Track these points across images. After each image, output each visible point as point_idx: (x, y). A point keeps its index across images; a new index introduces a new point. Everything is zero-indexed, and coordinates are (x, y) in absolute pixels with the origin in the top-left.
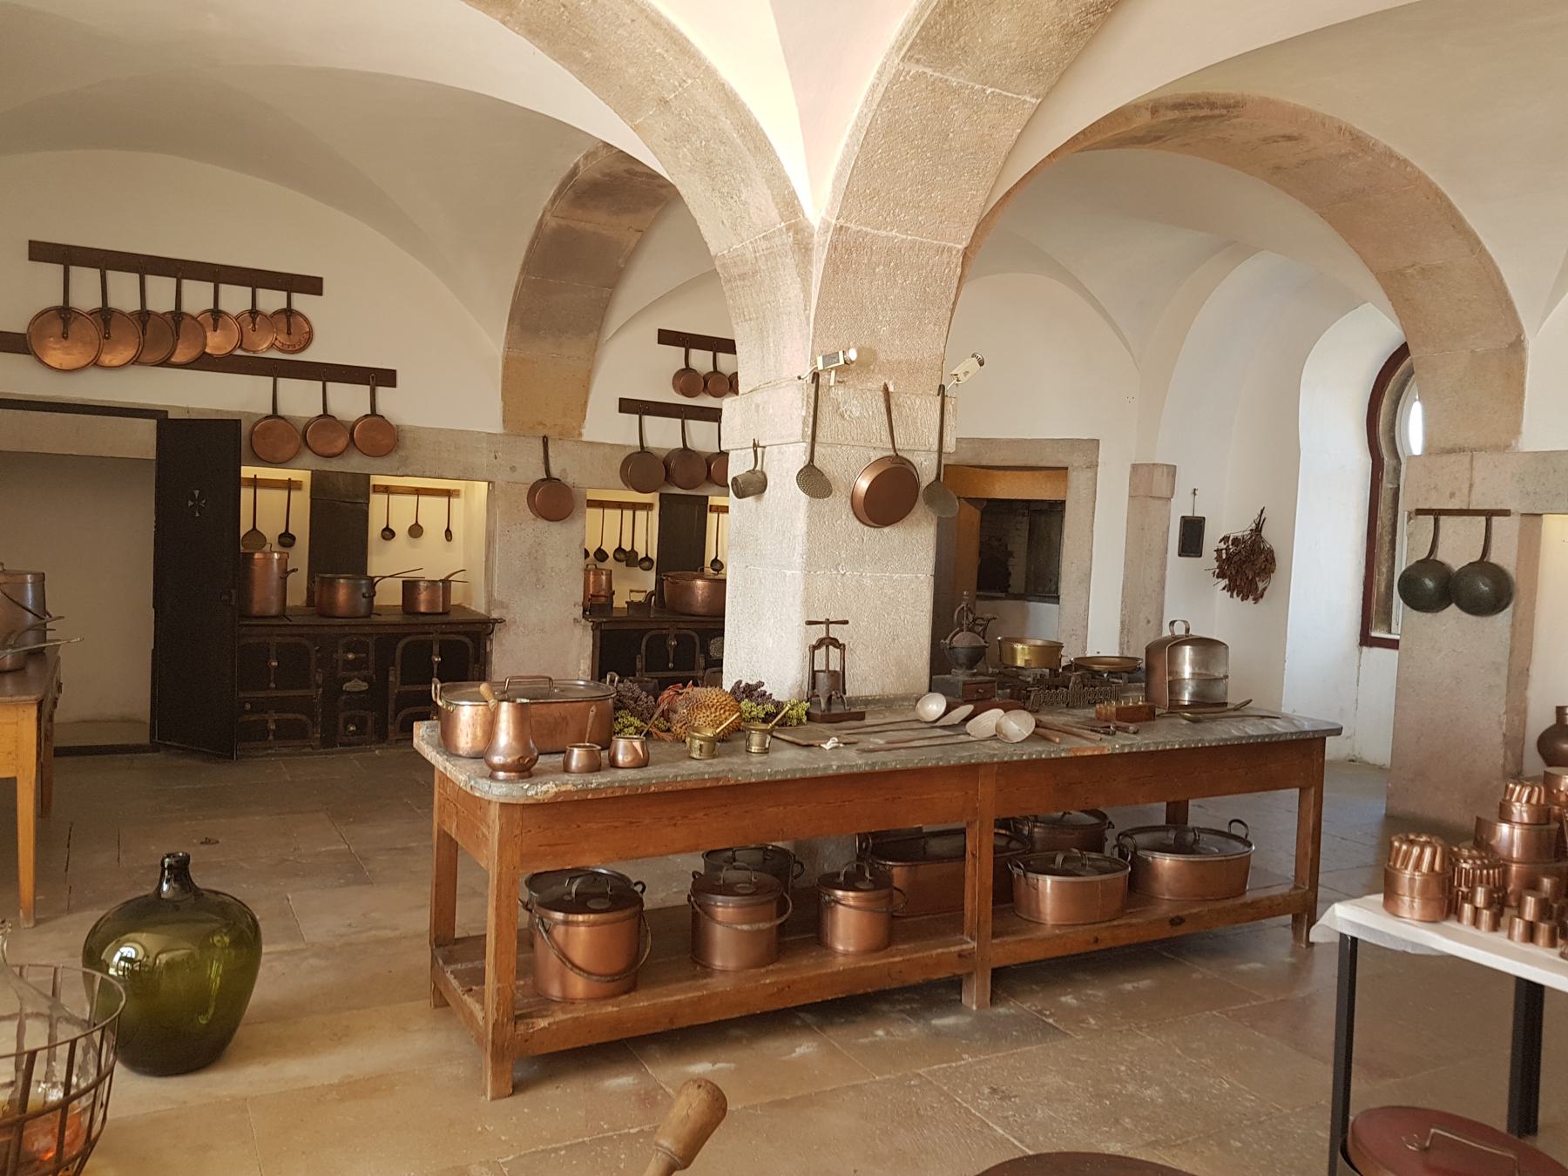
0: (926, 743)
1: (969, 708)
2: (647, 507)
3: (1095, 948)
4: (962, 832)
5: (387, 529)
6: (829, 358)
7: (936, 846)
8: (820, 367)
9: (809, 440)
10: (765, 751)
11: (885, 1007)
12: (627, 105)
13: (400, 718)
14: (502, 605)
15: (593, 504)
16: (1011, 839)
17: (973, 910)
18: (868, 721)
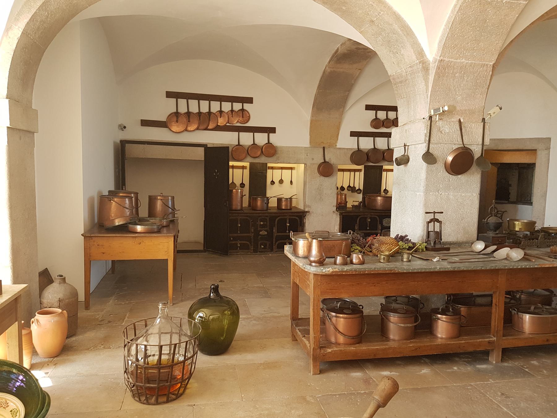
0: (476, 260)
1: (494, 247)
2: (359, 170)
4: (491, 296)
5: (272, 181)
6: (436, 110)
7: (479, 300)
8: (432, 114)
9: (427, 142)
10: (409, 261)
11: (457, 359)
12: (358, 25)
13: (277, 243)
14: (309, 207)
15: (340, 170)
16: (511, 299)
17: (495, 326)
18: (451, 251)
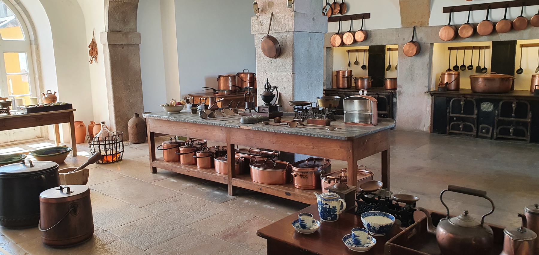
2: (487, 47)
3: (260, 191)
14: (400, 87)
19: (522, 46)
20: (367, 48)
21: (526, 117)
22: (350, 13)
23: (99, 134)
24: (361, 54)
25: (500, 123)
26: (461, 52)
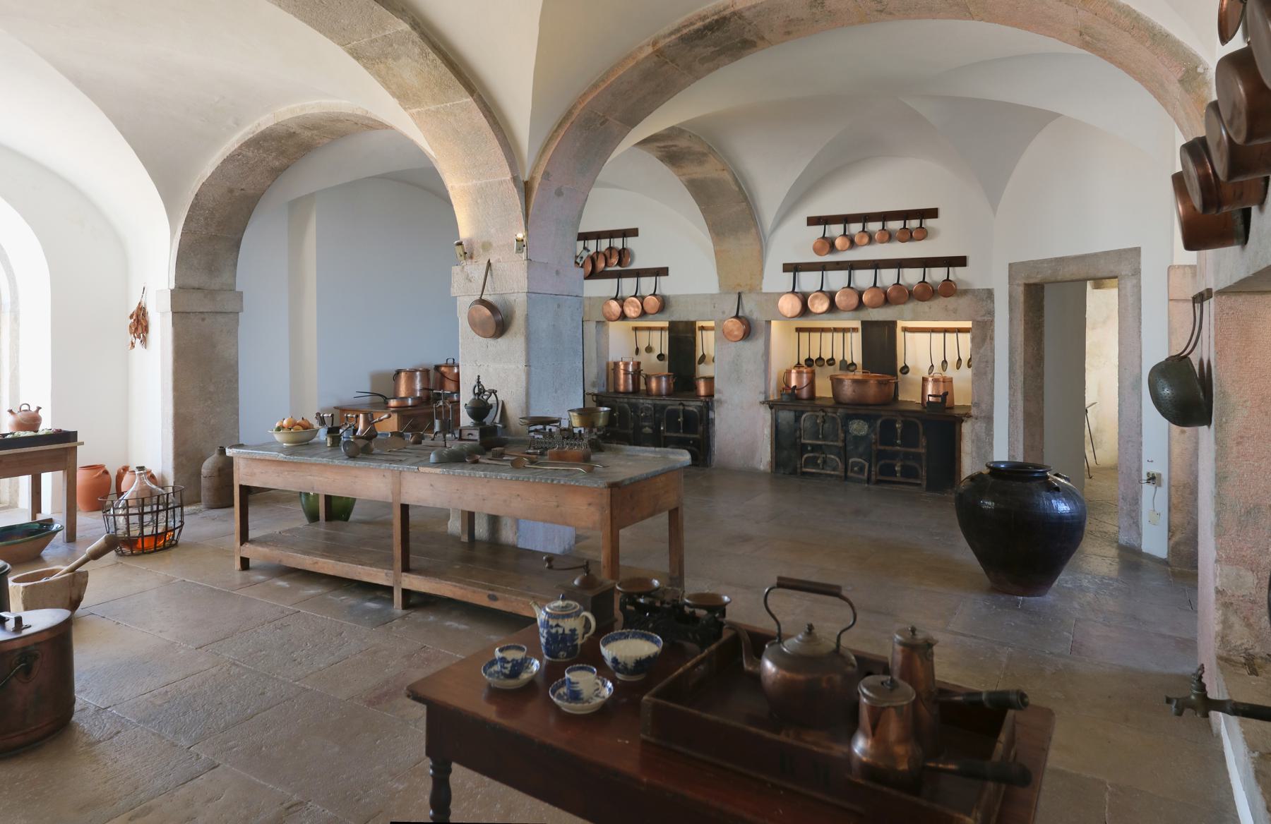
2: (855, 330)
14: (720, 392)
19: (905, 330)
20: (666, 324)
21: (916, 446)
22: (636, 265)
23: (131, 488)
24: (656, 334)
25: (881, 455)
26: (815, 336)
